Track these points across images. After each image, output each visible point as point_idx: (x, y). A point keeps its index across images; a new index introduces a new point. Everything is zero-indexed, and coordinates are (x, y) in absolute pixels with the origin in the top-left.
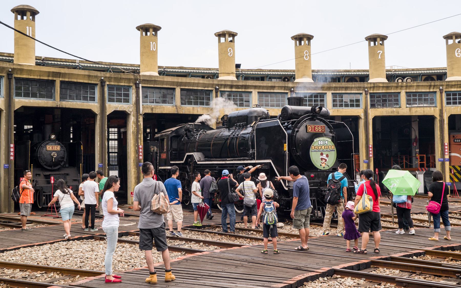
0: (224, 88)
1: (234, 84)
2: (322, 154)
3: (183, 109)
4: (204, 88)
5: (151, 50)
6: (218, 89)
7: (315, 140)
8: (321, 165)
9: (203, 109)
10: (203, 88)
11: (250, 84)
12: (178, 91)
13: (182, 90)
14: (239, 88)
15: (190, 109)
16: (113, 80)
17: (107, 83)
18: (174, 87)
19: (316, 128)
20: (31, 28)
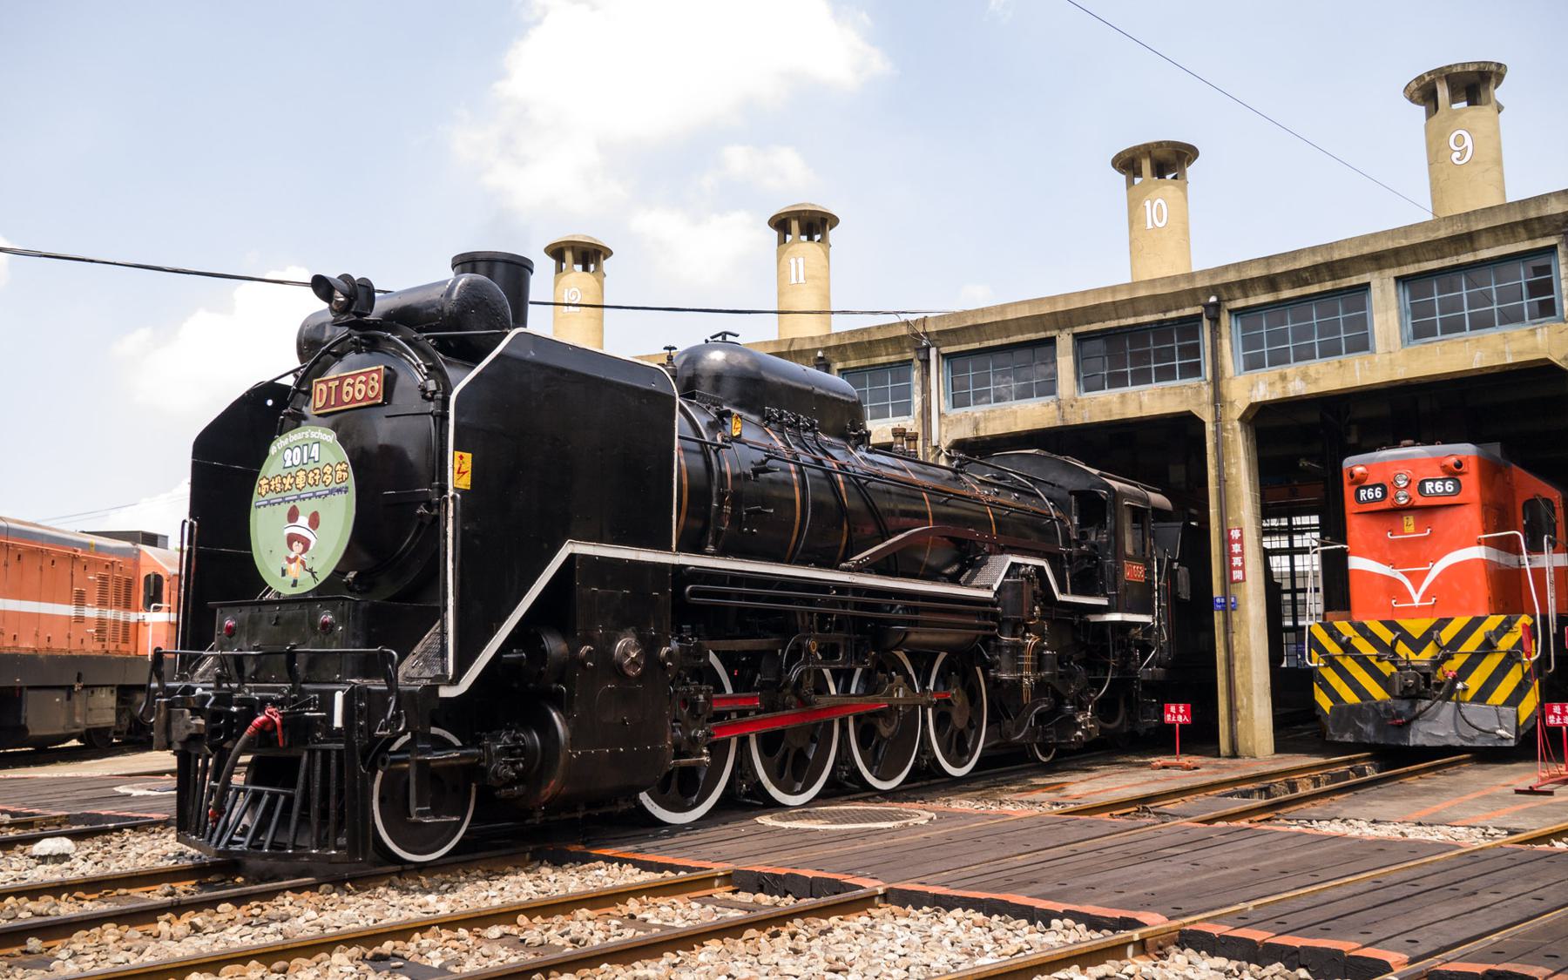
0: (1246, 296)
1: (1279, 270)
2: (293, 516)
3: (1083, 407)
4: (1164, 312)
5: (1150, 226)
6: (1217, 306)
7: (273, 450)
8: (284, 573)
9: (1162, 395)
10: (1161, 316)
11: (1347, 255)
12: (1065, 342)
13: (1079, 339)
14: (1307, 283)
15: (1110, 402)
16: (850, 353)
17: (839, 365)
18: (1049, 334)
19: (346, 388)
20: (801, 261)
